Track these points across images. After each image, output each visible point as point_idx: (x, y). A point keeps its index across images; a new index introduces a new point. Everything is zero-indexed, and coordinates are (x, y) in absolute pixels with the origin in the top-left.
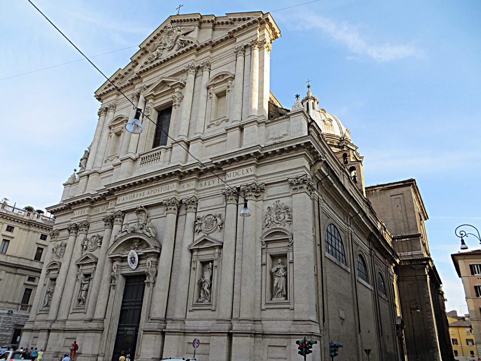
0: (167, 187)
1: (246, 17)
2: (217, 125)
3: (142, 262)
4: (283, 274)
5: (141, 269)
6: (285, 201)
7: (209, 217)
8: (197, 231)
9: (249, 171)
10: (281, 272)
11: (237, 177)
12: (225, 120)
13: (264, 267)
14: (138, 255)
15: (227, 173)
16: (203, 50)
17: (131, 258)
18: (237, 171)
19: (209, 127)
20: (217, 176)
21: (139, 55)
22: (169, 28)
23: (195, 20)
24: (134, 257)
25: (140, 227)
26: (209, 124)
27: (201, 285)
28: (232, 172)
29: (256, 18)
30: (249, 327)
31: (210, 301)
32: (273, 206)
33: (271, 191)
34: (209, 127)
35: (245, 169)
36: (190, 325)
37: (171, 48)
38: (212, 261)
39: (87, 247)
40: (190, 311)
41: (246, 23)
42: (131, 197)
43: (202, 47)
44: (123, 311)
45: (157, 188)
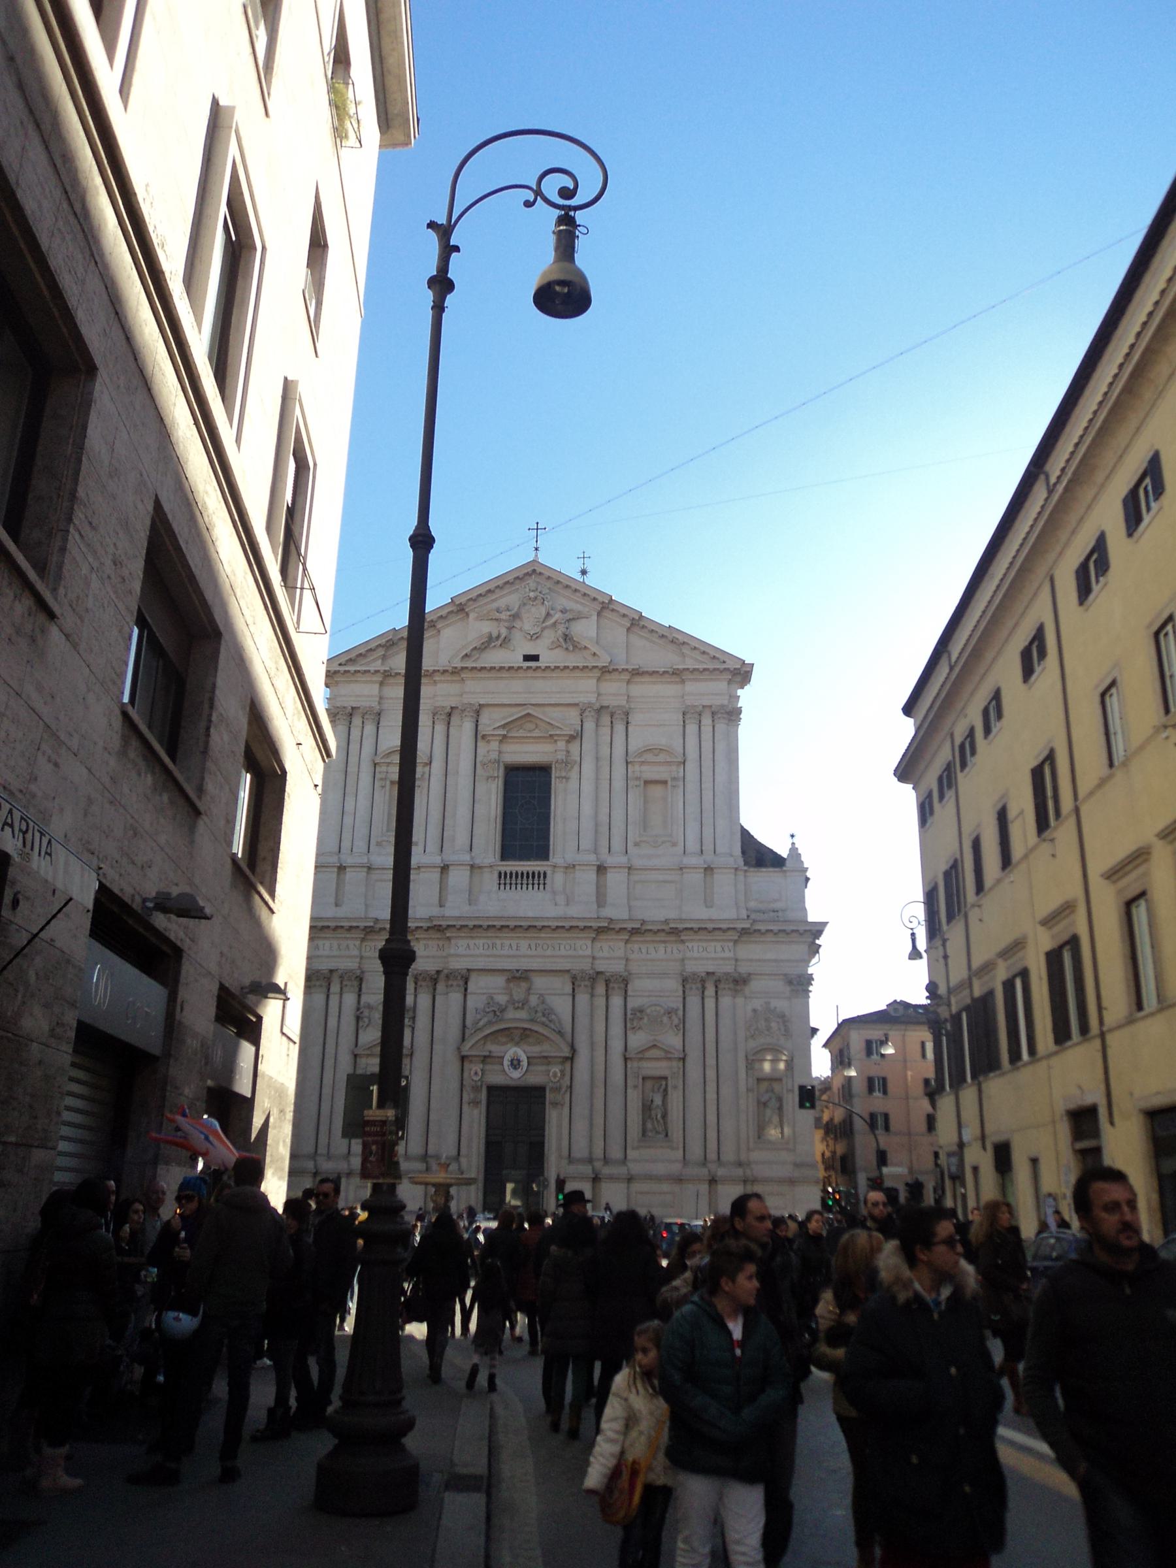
0: (573, 946)
1: (712, 653)
2: (654, 847)
3: (531, 1068)
4: (778, 1105)
5: (534, 1079)
6: (780, 1004)
7: (653, 1008)
8: (634, 1028)
9: (726, 949)
10: (774, 1103)
11: (704, 954)
12: (668, 841)
13: (750, 1094)
14: (528, 1058)
15: (687, 944)
16: (615, 676)
17: (512, 1061)
18: (705, 944)
19: (636, 844)
20: (664, 942)
21: (444, 613)
22: (533, 591)
23: (595, 599)
24: (519, 1061)
25: (517, 1005)
26: (638, 840)
27: (647, 1108)
28: (695, 944)
29: (731, 665)
30: (739, 1172)
31: (667, 1135)
32: (759, 1008)
33: (755, 985)
34: (636, 844)
35: (719, 945)
36: (635, 1168)
37: (535, 636)
38: (666, 1078)
39: (370, 1021)
40: (633, 1149)
41: (711, 666)
42: (486, 947)
43: (615, 670)
44: (489, 1144)
45: (549, 942)
